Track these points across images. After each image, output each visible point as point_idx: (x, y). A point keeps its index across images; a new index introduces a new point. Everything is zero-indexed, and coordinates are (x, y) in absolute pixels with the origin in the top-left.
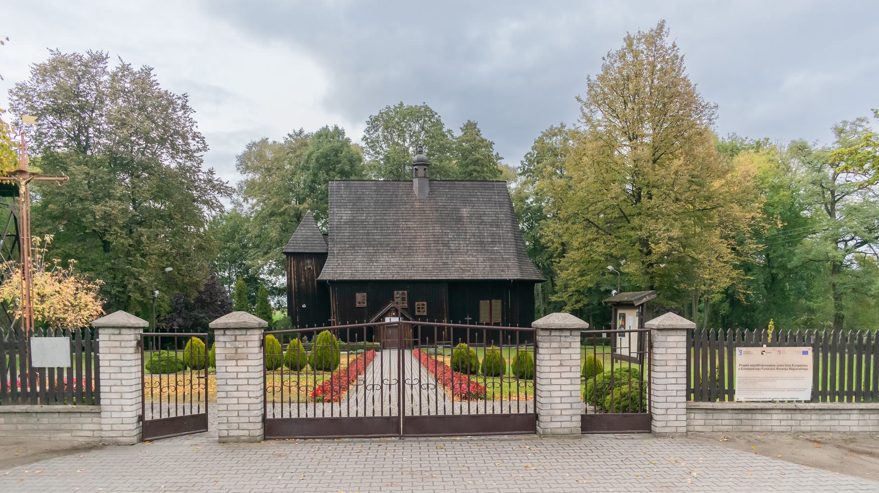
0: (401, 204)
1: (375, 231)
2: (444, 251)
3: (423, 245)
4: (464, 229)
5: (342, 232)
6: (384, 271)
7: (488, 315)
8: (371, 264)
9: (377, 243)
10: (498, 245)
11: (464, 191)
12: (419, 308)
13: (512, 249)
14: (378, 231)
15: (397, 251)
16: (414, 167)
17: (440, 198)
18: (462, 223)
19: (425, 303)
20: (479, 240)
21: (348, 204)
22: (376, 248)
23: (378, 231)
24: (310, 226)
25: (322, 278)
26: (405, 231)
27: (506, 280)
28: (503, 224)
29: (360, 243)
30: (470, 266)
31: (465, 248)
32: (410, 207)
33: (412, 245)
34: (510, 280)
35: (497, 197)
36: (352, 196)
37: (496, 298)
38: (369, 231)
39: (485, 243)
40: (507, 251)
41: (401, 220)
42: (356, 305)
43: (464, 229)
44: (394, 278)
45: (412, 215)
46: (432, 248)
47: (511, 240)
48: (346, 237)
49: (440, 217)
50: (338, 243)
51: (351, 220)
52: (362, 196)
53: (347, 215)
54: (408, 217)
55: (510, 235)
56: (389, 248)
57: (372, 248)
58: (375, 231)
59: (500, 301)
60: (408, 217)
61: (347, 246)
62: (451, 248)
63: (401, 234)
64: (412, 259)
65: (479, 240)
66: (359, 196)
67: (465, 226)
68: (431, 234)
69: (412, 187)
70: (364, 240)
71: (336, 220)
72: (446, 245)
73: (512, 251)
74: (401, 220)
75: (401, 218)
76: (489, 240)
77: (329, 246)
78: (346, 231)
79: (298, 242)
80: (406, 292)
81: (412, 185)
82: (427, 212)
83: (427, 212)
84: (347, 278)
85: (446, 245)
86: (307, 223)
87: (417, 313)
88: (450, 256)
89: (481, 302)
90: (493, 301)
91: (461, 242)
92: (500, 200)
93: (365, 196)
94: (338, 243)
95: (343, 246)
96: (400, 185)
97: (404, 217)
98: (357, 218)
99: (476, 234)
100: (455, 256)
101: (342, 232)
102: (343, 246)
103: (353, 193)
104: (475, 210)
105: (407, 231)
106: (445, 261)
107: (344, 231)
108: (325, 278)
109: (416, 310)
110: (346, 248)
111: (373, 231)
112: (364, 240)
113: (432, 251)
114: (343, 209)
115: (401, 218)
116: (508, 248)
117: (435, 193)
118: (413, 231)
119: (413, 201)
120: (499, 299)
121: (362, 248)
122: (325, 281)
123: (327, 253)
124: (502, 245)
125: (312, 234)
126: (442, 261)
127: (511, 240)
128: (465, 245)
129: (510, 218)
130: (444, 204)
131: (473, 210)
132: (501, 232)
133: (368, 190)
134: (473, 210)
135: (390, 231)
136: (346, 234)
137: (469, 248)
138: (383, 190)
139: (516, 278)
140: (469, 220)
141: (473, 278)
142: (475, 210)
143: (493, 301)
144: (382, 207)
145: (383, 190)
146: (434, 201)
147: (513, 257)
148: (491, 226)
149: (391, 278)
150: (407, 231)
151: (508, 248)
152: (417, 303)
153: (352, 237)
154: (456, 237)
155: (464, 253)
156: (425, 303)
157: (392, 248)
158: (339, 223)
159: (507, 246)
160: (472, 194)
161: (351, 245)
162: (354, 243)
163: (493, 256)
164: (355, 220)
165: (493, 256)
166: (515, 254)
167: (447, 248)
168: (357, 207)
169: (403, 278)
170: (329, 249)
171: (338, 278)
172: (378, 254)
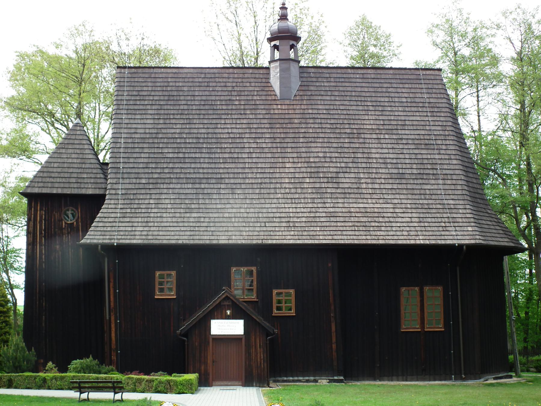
0: (247, 107)
1: (197, 155)
2: (329, 190)
3: (287, 181)
4: (366, 151)
5: (135, 155)
6: (212, 229)
7: (416, 316)
8: (188, 215)
9: (202, 176)
10: (433, 182)
11: (364, 85)
12: (279, 302)
13: (459, 187)
14: (203, 155)
15: (239, 191)
16: (273, 43)
17: (320, 98)
18: (361, 140)
19: (292, 291)
20: (396, 171)
21: (149, 107)
22: (197, 186)
23: (203, 155)
24: (77, 146)
25: (88, 241)
26: (254, 155)
27: (453, 246)
28: (439, 142)
29: (168, 176)
30: (381, 220)
31: (370, 186)
32: (264, 112)
33: (267, 181)
34: (461, 246)
35: (426, 96)
36: (157, 93)
37: (434, 283)
38: (187, 156)
39: (407, 176)
40: (450, 192)
41: (247, 136)
42: (154, 294)
43: (366, 151)
44: (231, 242)
45: (267, 126)
46: (306, 186)
47: (457, 172)
48: (141, 166)
49: (320, 130)
50: (126, 176)
51: (154, 136)
52: (175, 93)
53: (147, 126)
54: (259, 131)
55: (455, 162)
56: (223, 186)
57: (190, 186)
58: (197, 155)
59: (440, 288)
60: (259, 131)
61: (144, 181)
62: (341, 185)
63: (247, 160)
64: (267, 206)
65: (396, 171)
66: (171, 93)
67: (367, 146)
68: (303, 160)
69: (269, 78)
70: (175, 171)
71: (125, 136)
72: (334, 179)
73: (459, 192)
74: (247, 136)
75: (248, 131)
76: (415, 171)
77: (109, 182)
78: (143, 155)
79: (53, 175)
80: (254, 269)
81: (269, 74)
82: (296, 121)
83: (296, 121)
84: (140, 242)
85: (334, 179)
86: (71, 141)
87: (275, 312)
88: (340, 201)
89: (403, 289)
90: (426, 289)
91: (362, 176)
92: (432, 100)
93: (181, 93)
94: (126, 176)
95: (134, 181)
96: (246, 76)
97: (253, 131)
98: (164, 131)
99: (388, 161)
100: (351, 200)
101: (135, 155)
102: (134, 181)
103: (159, 89)
104: (386, 118)
105: (258, 155)
106: (332, 210)
107: (138, 155)
108: (95, 241)
109: (275, 305)
110: (141, 186)
111: (193, 155)
112: (175, 171)
113: (305, 191)
114: (138, 117)
115: (248, 131)
116: (453, 187)
117: (312, 88)
118: (269, 155)
119: (269, 102)
120: (437, 284)
121: (172, 186)
122: (96, 246)
123: (104, 196)
124: (441, 182)
125: (79, 161)
126: (325, 210)
127: (457, 172)
128: (369, 181)
129: (451, 133)
130: (327, 107)
131: (381, 118)
132: (437, 157)
133: (187, 84)
134: (381, 118)
135: (227, 155)
136: (142, 160)
137: (377, 186)
138: (214, 84)
139: (473, 242)
140: (374, 136)
141: (387, 242)
142: (386, 118)
143: (426, 289)
144: (211, 112)
145: (214, 84)
146: (309, 102)
147: (461, 202)
148: (418, 146)
149: (226, 242)
150: (258, 155)
151: (453, 187)
152: (275, 292)
153: (153, 166)
154: (350, 165)
155: (369, 196)
156: (292, 291)
157: (229, 186)
158: (130, 141)
159: (449, 182)
160: (380, 90)
161: (151, 181)
162: (156, 176)
163: (425, 202)
164: (160, 136)
165: (425, 202)
166: (466, 197)
167: (335, 185)
168: (166, 112)
169: (249, 242)
170: (109, 187)
171: (121, 241)
172: (201, 196)
